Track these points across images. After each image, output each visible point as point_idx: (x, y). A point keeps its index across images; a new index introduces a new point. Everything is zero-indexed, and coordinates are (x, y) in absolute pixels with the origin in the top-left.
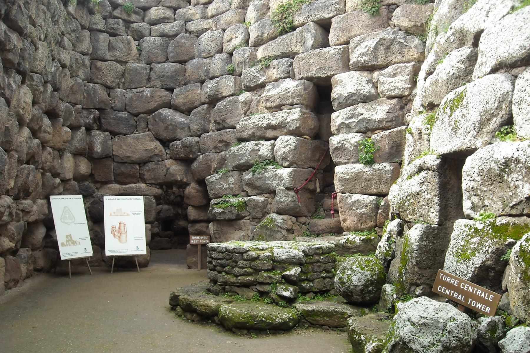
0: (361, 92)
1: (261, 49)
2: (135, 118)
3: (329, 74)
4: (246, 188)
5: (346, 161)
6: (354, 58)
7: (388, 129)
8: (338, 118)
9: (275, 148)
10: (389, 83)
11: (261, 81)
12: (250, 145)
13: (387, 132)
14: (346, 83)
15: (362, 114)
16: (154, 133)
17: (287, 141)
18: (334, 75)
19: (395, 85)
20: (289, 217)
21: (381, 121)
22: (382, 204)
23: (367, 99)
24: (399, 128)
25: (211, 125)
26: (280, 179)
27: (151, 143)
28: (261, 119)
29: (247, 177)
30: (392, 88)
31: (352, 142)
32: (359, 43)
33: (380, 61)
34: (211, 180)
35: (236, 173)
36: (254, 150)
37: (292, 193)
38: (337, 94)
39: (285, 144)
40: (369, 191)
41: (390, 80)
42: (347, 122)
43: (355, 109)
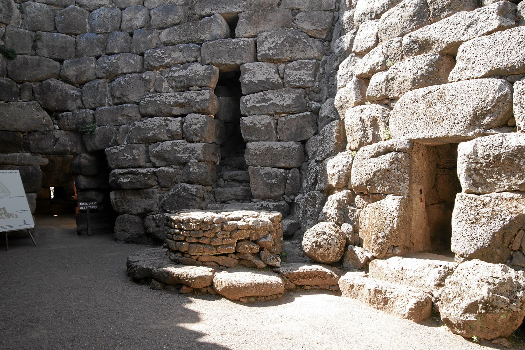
0: (271, 80)
1: (164, 33)
2: (19, 86)
3: (238, 62)
4: (153, 160)
5: (256, 139)
6: (262, 50)
7: (293, 114)
8: (248, 101)
9: (185, 124)
10: (295, 75)
11: (166, 61)
12: (158, 121)
13: (294, 116)
14: (255, 72)
15: (272, 100)
16: (41, 103)
17: (197, 119)
18: (242, 64)
19: (300, 77)
20: (201, 186)
21: (289, 106)
22: (290, 175)
23: (274, 87)
24: (305, 113)
25: (107, 100)
26: (193, 151)
27: (38, 113)
28: (168, 98)
29: (155, 149)
30: (297, 80)
31: (263, 123)
32: (266, 38)
33: (287, 56)
34: (113, 151)
35: (142, 147)
36: (161, 125)
37: (203, 165)
38: (247, 80)
39: (196, 121)
40: (278, 165)
41: (295, 72)
42: (258, 105)
43: (265, 94)
